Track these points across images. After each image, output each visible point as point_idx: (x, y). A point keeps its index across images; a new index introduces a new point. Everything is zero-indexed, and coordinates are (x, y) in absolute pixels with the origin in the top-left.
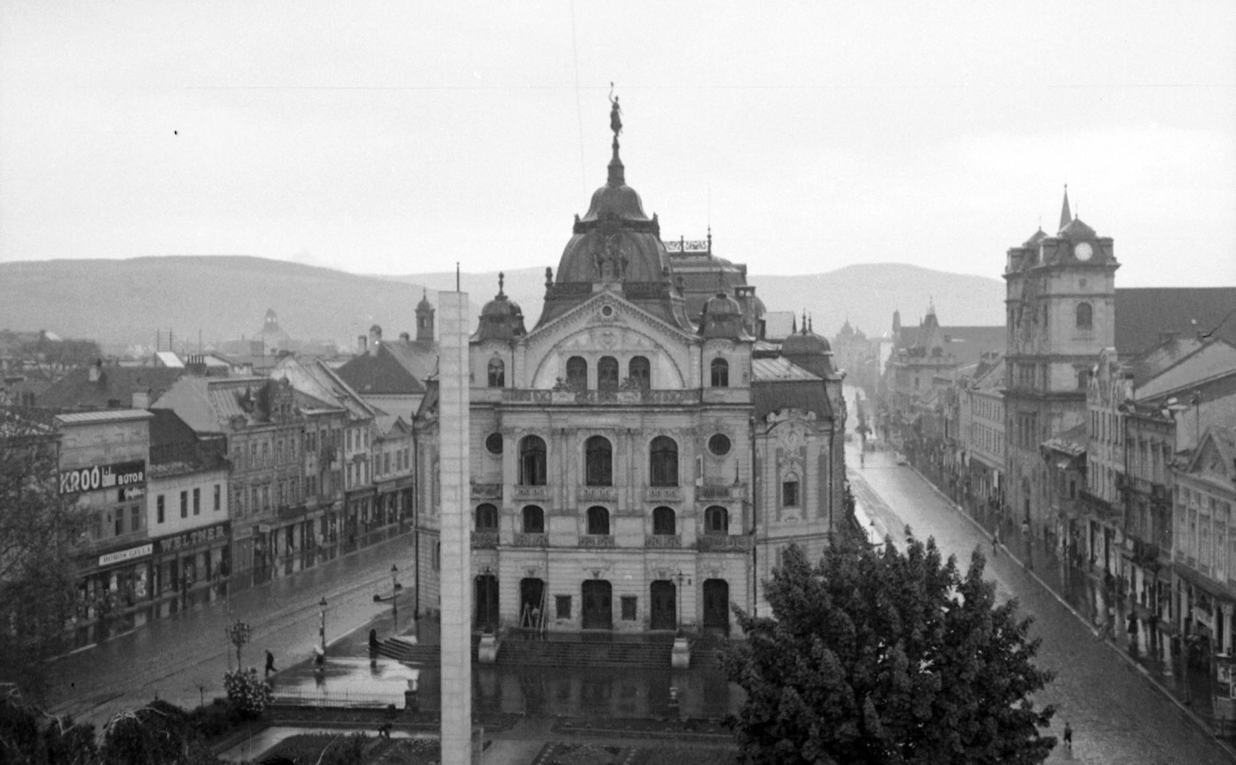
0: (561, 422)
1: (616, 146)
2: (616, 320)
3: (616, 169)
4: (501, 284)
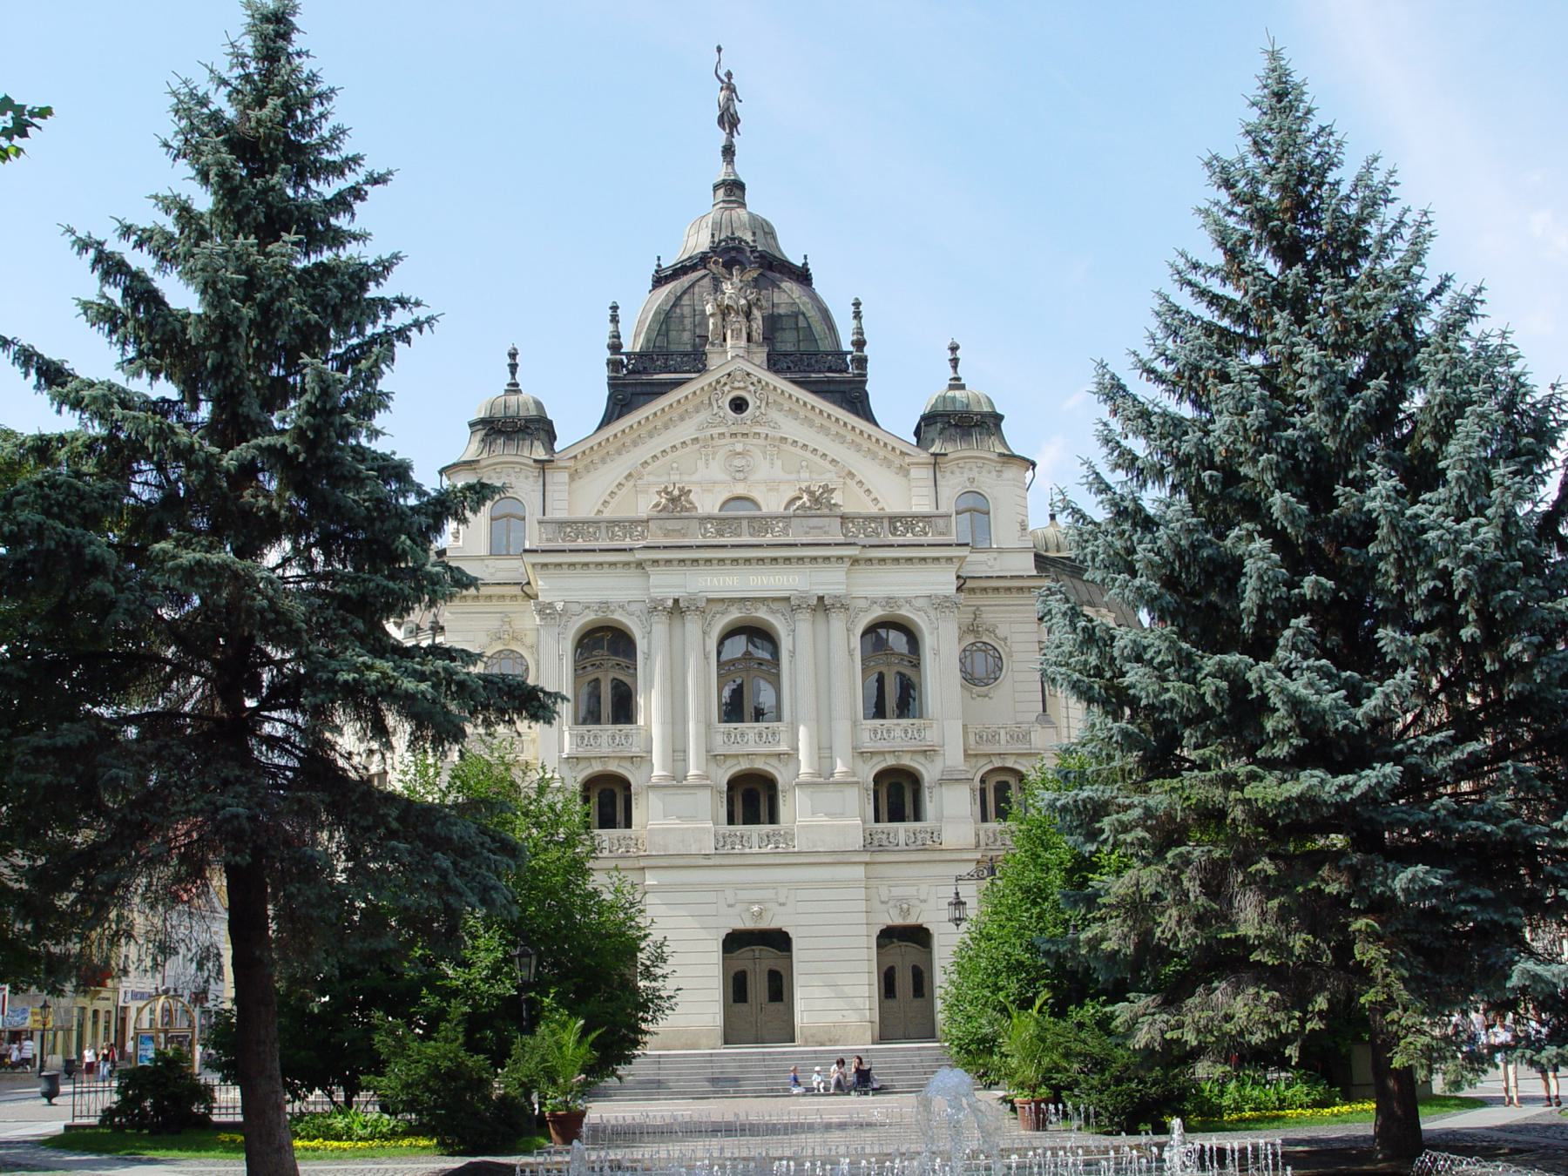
0: (668, 584)
1: (728, 152)
4: (513, 368)
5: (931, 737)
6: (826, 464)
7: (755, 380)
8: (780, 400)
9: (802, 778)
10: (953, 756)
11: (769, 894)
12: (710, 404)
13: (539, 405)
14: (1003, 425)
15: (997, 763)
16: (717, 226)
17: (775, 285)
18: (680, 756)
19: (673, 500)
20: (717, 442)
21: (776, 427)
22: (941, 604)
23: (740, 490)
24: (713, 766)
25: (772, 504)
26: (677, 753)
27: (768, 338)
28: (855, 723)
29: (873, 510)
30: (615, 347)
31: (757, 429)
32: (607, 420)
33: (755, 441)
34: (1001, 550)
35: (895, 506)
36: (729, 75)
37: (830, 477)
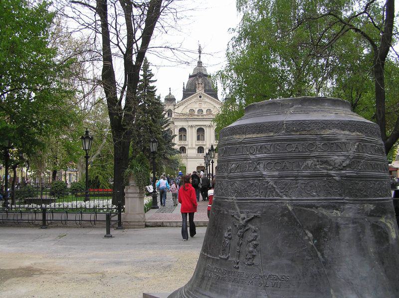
0: (191, 123)
3: (200, 63)
26: (192, 145)
27: (205, 87)
30: (184, 89)
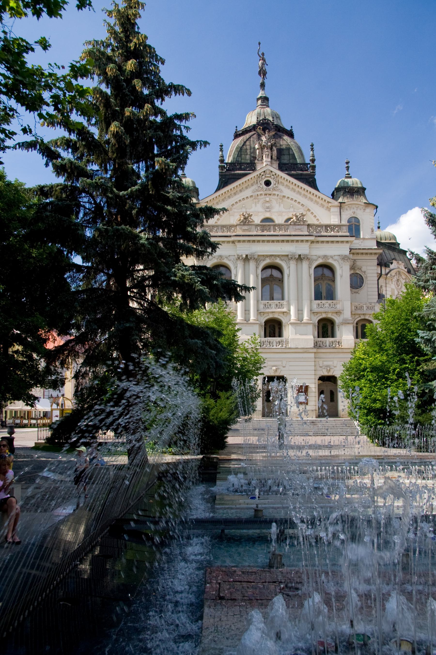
1: (263, 85)
2: (274, 189)
5: (339, 307)
6: (300, 206)
7: (274, 174)
8: (283, 181)
9: (292, 321)
10: (347, 314)
11: (279, 363)
12: (257, 183)
13: (193, 183)
14: (366, 192)
15: (362, 317)
16: (259, 115)
17: (280, 137)
18: (247, 312)
19: (245, 218)
20: (259, 197)
21: (281, 191)
22: (344, 258)
23: (268, 215)
24: (259, 316)
25: (279, 220)
28: (311, 301)
29: (316, 223)
30: (222, 161)
31: (274, 192)
32: (218, 189)
33: (274, 197)
34: (364, 239)
35: (325, 221)
36: (263, 54)
37: (300, 211)
